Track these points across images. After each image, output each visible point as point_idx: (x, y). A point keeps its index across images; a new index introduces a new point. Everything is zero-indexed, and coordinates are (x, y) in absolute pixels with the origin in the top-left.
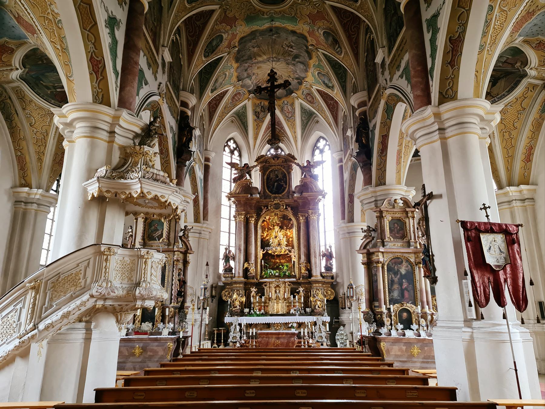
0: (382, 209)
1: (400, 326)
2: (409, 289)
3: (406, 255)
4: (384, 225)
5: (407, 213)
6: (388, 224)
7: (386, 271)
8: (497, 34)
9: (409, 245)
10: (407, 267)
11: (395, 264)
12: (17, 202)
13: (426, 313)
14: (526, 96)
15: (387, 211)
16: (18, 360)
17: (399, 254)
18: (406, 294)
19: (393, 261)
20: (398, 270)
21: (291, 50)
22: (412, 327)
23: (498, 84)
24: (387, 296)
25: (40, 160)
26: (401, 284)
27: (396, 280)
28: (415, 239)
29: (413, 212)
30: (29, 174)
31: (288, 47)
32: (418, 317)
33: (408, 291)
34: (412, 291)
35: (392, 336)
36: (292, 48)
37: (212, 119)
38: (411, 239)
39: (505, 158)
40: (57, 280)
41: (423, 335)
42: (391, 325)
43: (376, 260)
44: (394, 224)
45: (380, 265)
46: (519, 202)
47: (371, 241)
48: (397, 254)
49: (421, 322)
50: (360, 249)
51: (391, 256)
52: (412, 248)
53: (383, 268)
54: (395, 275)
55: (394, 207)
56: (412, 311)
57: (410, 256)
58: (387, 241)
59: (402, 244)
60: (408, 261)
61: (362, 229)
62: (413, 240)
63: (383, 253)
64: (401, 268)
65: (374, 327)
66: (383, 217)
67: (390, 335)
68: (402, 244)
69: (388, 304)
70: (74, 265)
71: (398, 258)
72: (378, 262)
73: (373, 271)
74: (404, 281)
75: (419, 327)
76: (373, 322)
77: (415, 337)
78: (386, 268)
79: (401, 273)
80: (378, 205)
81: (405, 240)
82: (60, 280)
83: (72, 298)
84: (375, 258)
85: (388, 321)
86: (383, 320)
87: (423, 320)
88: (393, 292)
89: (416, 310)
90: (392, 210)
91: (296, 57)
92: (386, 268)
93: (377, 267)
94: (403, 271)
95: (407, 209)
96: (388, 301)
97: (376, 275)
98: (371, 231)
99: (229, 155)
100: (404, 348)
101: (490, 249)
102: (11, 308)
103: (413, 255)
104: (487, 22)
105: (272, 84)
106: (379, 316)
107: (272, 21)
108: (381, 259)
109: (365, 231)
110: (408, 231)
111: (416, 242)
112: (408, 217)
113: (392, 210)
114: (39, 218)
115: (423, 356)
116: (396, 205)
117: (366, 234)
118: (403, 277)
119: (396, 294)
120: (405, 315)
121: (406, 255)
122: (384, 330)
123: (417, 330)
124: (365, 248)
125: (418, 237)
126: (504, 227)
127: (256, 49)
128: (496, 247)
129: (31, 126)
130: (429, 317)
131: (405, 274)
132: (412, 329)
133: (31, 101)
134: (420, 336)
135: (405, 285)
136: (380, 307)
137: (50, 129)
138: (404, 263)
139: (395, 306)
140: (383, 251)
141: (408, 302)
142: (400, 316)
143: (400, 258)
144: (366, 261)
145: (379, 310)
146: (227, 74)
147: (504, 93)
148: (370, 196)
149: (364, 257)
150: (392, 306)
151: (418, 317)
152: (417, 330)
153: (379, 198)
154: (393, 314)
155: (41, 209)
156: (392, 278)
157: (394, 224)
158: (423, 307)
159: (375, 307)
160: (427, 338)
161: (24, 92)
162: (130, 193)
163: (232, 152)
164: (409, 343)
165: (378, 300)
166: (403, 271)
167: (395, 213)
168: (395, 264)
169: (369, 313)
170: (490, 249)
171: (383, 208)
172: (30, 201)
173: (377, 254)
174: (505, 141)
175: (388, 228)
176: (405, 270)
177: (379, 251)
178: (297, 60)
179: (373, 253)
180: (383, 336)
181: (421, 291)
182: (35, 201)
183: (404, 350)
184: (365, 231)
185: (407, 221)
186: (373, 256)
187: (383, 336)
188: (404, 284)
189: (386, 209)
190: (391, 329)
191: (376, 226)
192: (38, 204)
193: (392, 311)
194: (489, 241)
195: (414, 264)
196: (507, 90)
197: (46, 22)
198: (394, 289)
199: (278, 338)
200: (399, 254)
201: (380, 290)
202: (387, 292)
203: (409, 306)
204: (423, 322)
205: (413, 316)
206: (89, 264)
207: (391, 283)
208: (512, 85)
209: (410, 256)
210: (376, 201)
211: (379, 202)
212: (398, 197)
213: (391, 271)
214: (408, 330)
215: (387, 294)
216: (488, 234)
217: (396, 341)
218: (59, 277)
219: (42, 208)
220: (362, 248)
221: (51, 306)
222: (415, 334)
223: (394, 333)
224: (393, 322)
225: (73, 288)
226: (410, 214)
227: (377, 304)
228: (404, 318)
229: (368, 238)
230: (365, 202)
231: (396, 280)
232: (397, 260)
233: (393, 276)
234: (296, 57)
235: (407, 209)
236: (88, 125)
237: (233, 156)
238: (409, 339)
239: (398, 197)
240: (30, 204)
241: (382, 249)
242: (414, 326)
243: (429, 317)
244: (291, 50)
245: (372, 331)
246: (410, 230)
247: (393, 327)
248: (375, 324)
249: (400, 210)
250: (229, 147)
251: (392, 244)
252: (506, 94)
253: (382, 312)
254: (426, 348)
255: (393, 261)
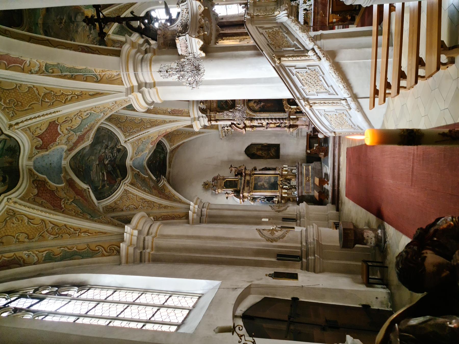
12: (201, 222)
16: (338, 59)
21: (64, 21)
25: (166, 207)
30: (178, 214)
31: (61, 23)
36: (62, 20)
40: (273, 45)
70: (262, 37)
82: (273, 43)
83: (289, 33)
91: (70, 18)
102: (295, 78)
107: (37, 24)
114: (213, 207)
129: (136, 209)
133: (115, 202)
137: (139, 196)
155: (207, 206)
161: (107, 206)
162: (200, 15)
172: (200, 213)
178: (73, 19)
182: (200, 210)
192: (203, 207)
197: (47, 100)
199: (318, 13)
206: (260, 27)
218: (270, 44)
219: (206, 205)
221: (295, 46)
225: (281, 34)
234: (70, 18)
236: (140, 65)
240: (203, 213)
244: (64, 21)
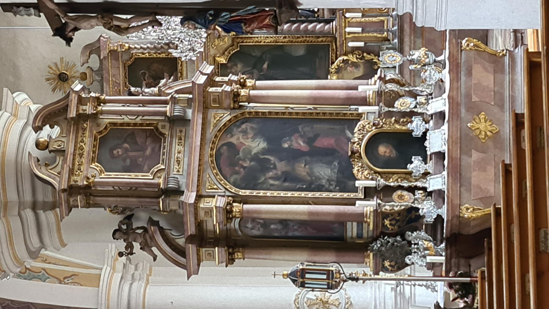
0: (64, 186)
1: (416, 164)
2: (311, 135)
3: (211, 131)
4: (113, 184)
5: (82, 118)
6: (113, 174)
7: (255, 193)
9: (179, 122)
10: (245, 132)
11: (237, 164)
13: (379, 94)
15: (71, 172)
17: (208, 151)
18: (323, 142)
19: (226, 170)
20: (255, 158)
22: (418, 133)
24: (331, 195)
26: (294, 155)
27: (281, 166)
28: (166, 102)
29: (81, 101)
32: (389, 114)
33: (316, 136)
34: (318, 127)
35: (445, 188)
38: (164, 114)
41: (439, 105)
42: (412, 190)
43: (222, 217)
44: (113, 157)
45: (237, 207)
47: (162, 230)
48: (207, 158)
49: (403, 109)
50: (183, 266)
51: (211, 175)
52: (189, 112)
53: (245, 200)
54: (268, 169)
55: (61, 152)
56: (374, 130)
57: (213, 121)
58: (166, 180)
59: (175, 141)
60: (227, 129)
61: (121, 254)
62: (168, 109)
63: (199, 197)
65: (420, 238)
66: (88, 187)
67: (440, 193)
68: (175, 141)
69: (352, 195)
71: (218, 156)
72: (228, 212)
73: (255, 232)
74: (286, 146)
75: (417, 114)
76: (404, 239)
77: (445, 127)
78: (248, 192)
79: (264, 151)
80: (50, 199)
81: (166, 132)
84: (214, 223)
85: (401, 197)
86: (399, 213)
87: (397, 104)
89: (372, 117)
90: (70, 158)
92: (248, 192)
93: (244, 218)
94: (258, 145)
95: (72, 113)
96: (345, 195)
97: (266, 223)
98: (129, 225)
100: (475, 155)
103: (212, 113)
106: (387, 222)
108: (221, 202)
109: (130, 247)
110: (138, 120)
111: (175, 101)
112: (94, 117)
113: (70, 158)
115: (496, 110)
116: (55, 146)
117: (137, 246)
118: (274, 148)
119: (324, 172)
120: (383, 150)
121: (211, 131)
122: (428, 209)
123: (427, 122)
124: (182, 252)
125: (160, 94)
130: (391, 87)
131: (268, 140)
132: (425, 134)
134: (441, 115)
135: (301, 144)
136: (360, 218)
138: (233, 140)
139: (360, 175)
140: (194, 194)
141: (349, 140)
142: (388, 163)
143: (218, 151)
144: (223, 250)
145: (371, 221)
148: (16, 223)
149: (211, 257)
150: (357, 183)
151: (389, 114)
152: (427, 122)
153: (28, 197)
154: (382, 182)
157: (113, 157)
158: (364, 101)
159: (360, 236)
160: (445, 96)
164: (462, 141)
165: (341, 221)
166: (258, 145)
167: (78, 151)
168: (237, 164)
169: (379, 250)
171: (60, 183)
173: (202, 214)
175: (126, 175)
176: (253, 138)
177: (195, 205)
179: (199, 225)
180: (444, 211)
181: (315, 101)
183: (482, 155)
184: (130, 247)
185: (106, 120)
186: (210, 227)
187: (444, 211)
188: (295, 145)
189: (66, 175)
190: (424, 189)
191: (114, 210)
193: (372, 184)
195: (238, 112)
198: (310, 174)
200: (208, 151)
201: (311, 213)
202: (317, 194)
203: (359, 137)
204: (405, 104)
205: (386, 128)
207: (290, 180)
209: (213, 121)
210: (34, 207)
211: (40, 198)
212: (32, 137)
213: (256, 178)
214: (427, 144)
215: (324, 195)
217: (457, 174)
220: (182, 260)
222: (437, 126)
223: (436, 183)
224: (405, 184)
226: (89, 109)
227: (352, 230)
228: (394, 154)
229: (152, 238)
230: (35, 242)
231: (281, 166)
232: (224, 158)
233: (271, 174)
235: (72, 113)
238: (450, 141)
239: (32, 137)
241: (190, 197)
242: (417, 126)
243: (391, 87)
245: (431, 244)
246: (137, 114)
247: (419, 184)
248: (412, 236)
249: (72, 136)
251: (175, 167)
253: (375, 211)
255: (226, 170)
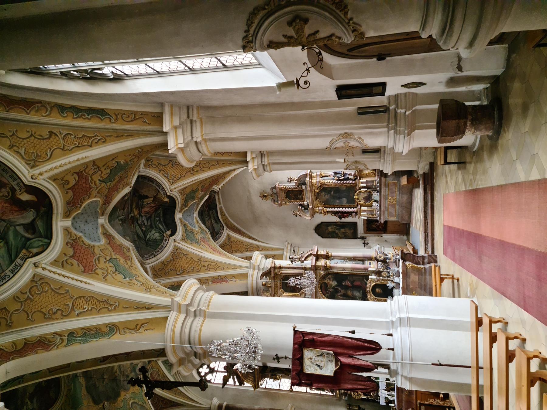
8: (98, 301)
10: (329, 279)
14: (157, 164)
18: (357, 283)
20: (333, 288)
23: (146, 194)
26: (346, 288)
27: (343, 291)
33: (354, 281)
37: (178, 404)
39: (219, 167)
46: (263, 159)
54: (339, 292)
55: (271, 287)
60: (324, 277)
64: (331, 285)
79: (336, 286)
88: (355, 296)
94: (334, 283)
99: (215, 374)
101: (319, 366)
104: (85, 333)
105: (143, 382)
118: (340, 284)
119: (357, 294)
120: (377, 290)
126: (296, 346)
127: (105, 377)
128: (317, 358)
131: (337, 281)
135: (349, 283)
138: (326, 281)
146: (131, 401)
147: (154, 185)
156: (340, 296)
163: (212, 371)
170: (319, 366)
174: (203, 169)
176: (333, 281)
194: (311, 365)
196: (151, 183)
198: (353, 295)
208: (146, 181)
216: (304, 365)
228: (381, 292)
233: (339, 294)
237: (216, 369)
250: (206, 374)
252: (155, 182)
254: (411, 287)
